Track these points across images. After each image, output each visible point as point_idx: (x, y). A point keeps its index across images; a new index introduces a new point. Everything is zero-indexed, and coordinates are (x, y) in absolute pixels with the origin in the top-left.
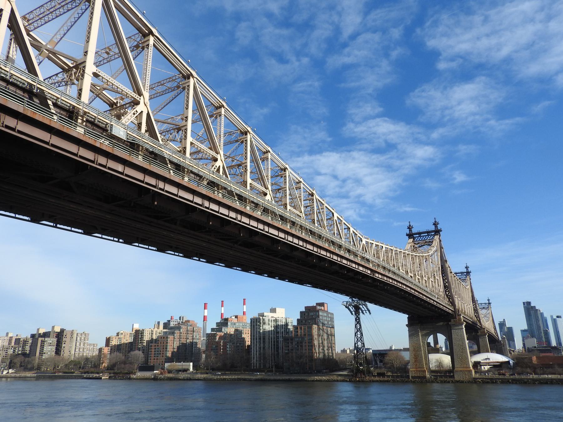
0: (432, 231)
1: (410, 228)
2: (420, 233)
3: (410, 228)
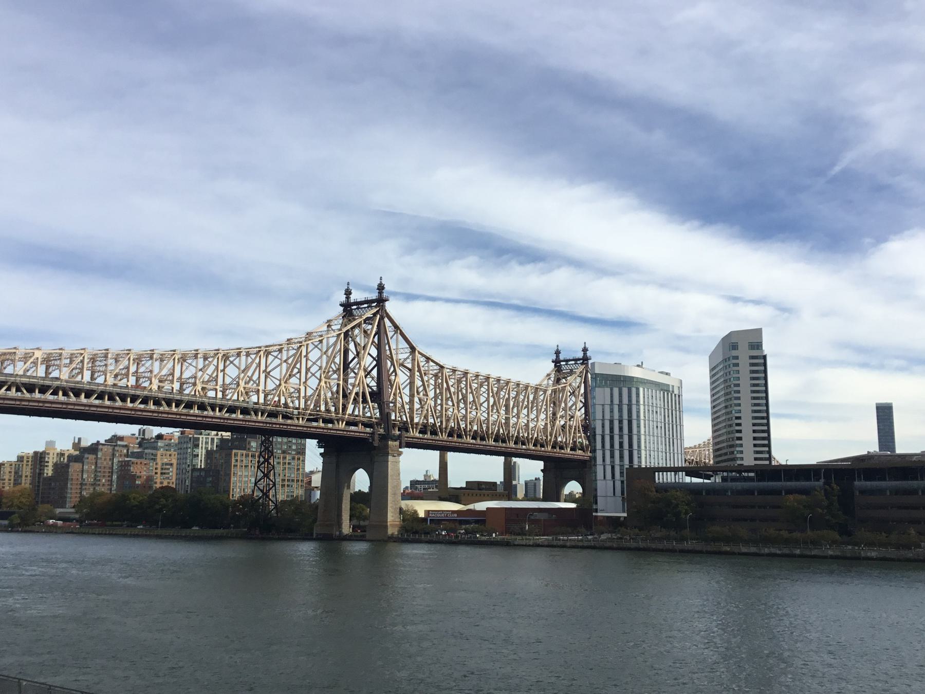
0: (372, 301)
1: (348, 293)
2: (358, 303)
3: (348, 293)
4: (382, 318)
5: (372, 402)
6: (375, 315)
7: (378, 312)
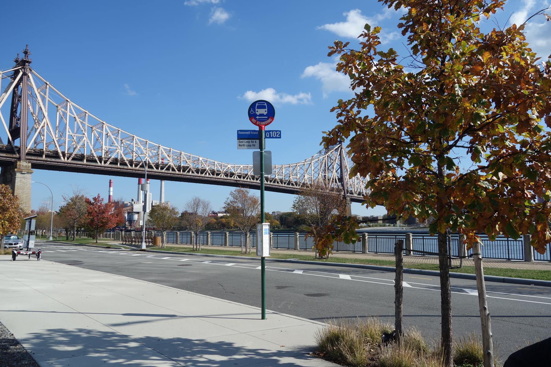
4: (341, 148)
5: (339, 182)
6: (339, 147)
7: (339, 146)
